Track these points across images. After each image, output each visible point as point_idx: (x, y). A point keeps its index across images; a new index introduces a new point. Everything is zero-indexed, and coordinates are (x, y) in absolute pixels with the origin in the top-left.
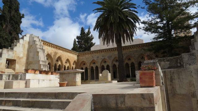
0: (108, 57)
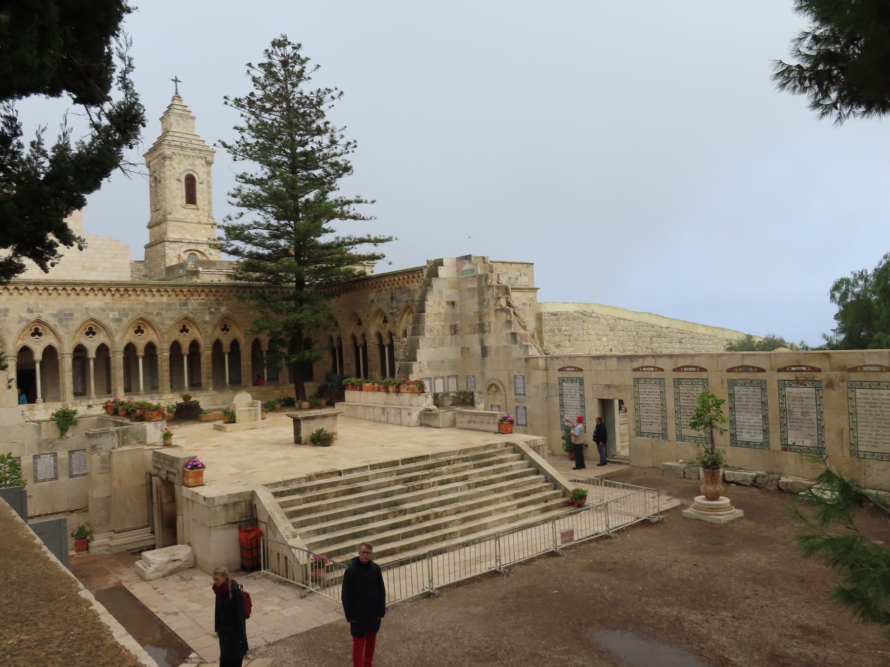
0: (55, 316)
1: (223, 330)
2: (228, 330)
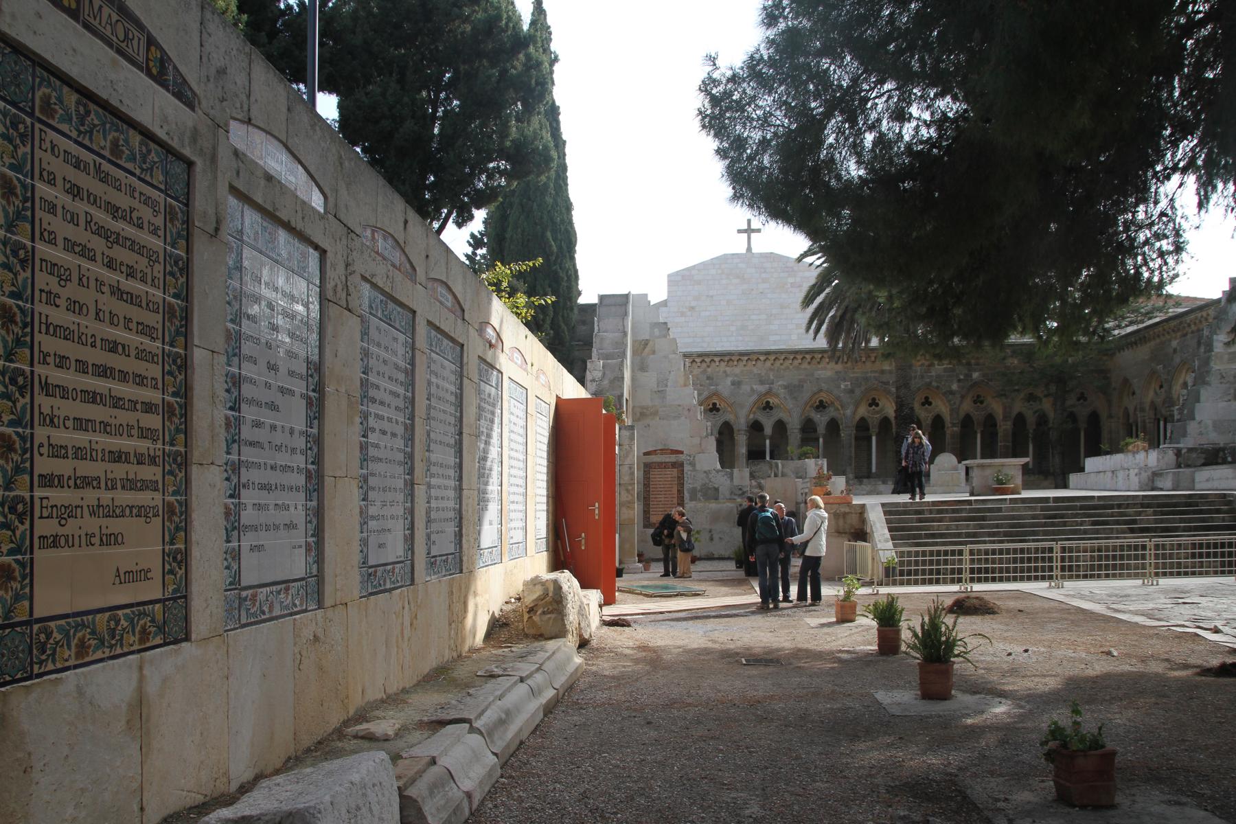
0: (786, 387)
1: (975, 402)
2: (982, 402)
